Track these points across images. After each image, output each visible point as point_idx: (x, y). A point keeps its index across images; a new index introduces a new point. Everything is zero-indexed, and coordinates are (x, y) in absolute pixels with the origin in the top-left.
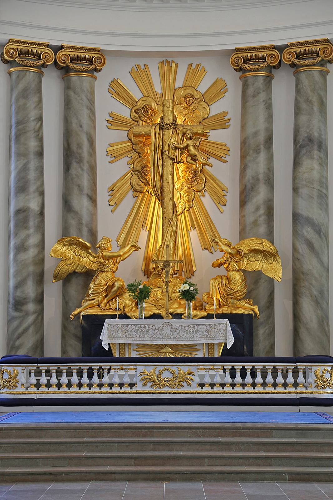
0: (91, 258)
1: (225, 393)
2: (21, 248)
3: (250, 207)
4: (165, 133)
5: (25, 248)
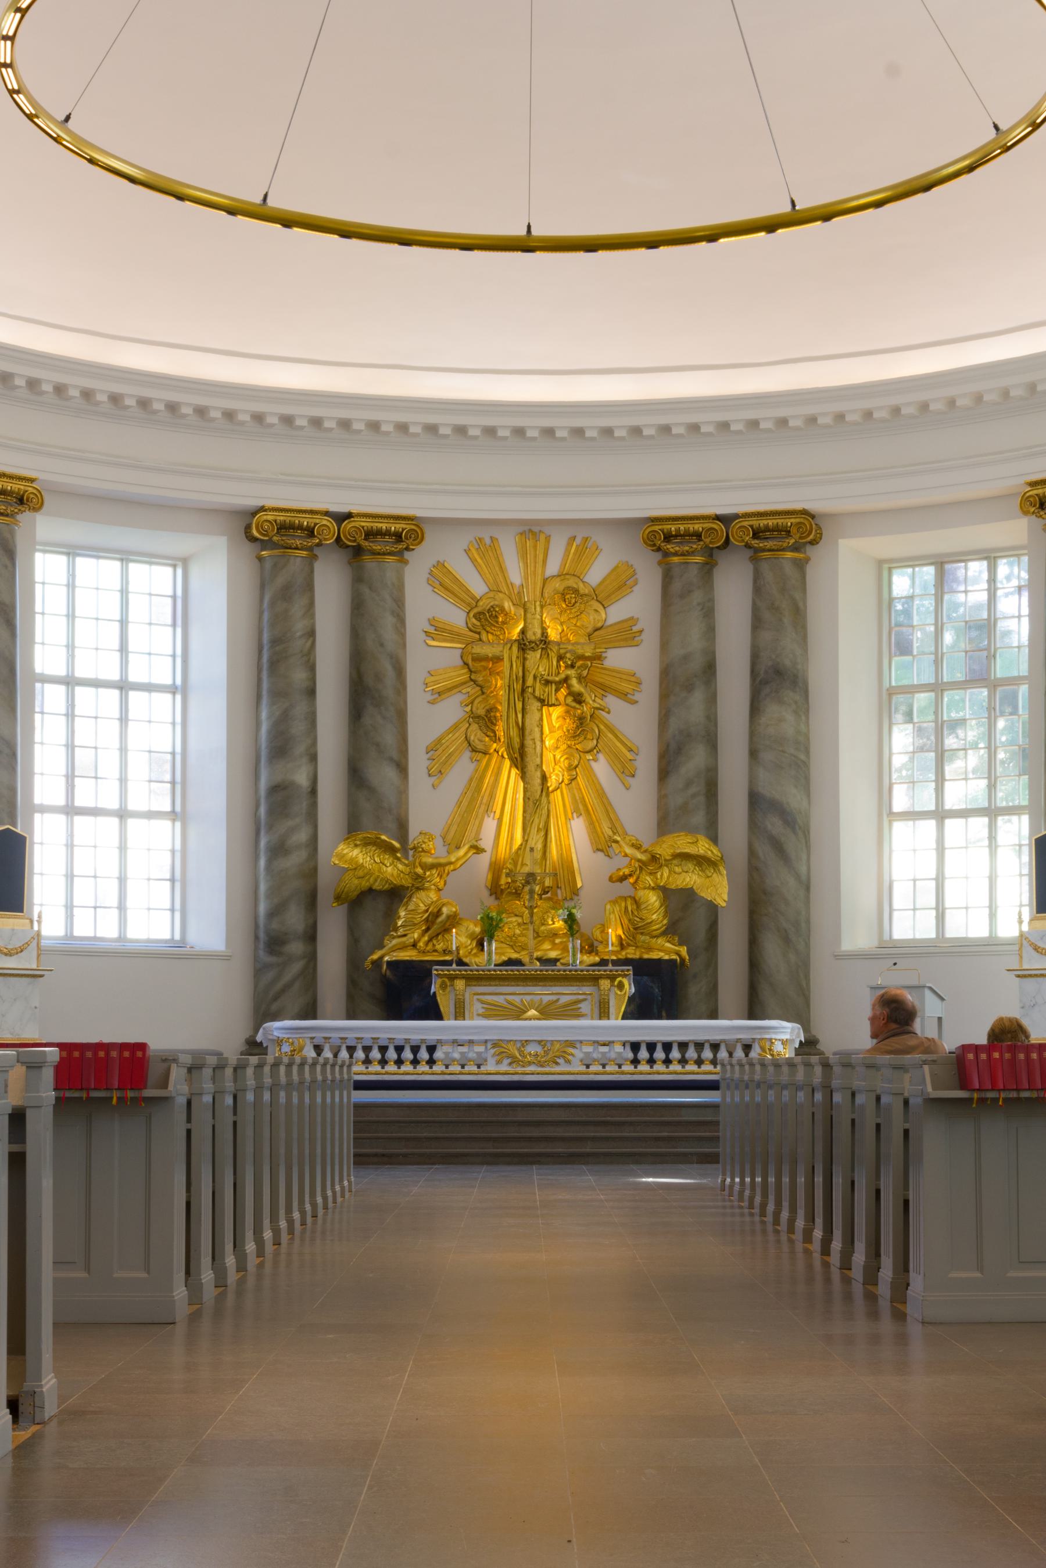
0: (400, 866)
1: (623, 1073)
2: (278, 850)
3: (675, 782)
4: (528, 656)
5: (286, 850)
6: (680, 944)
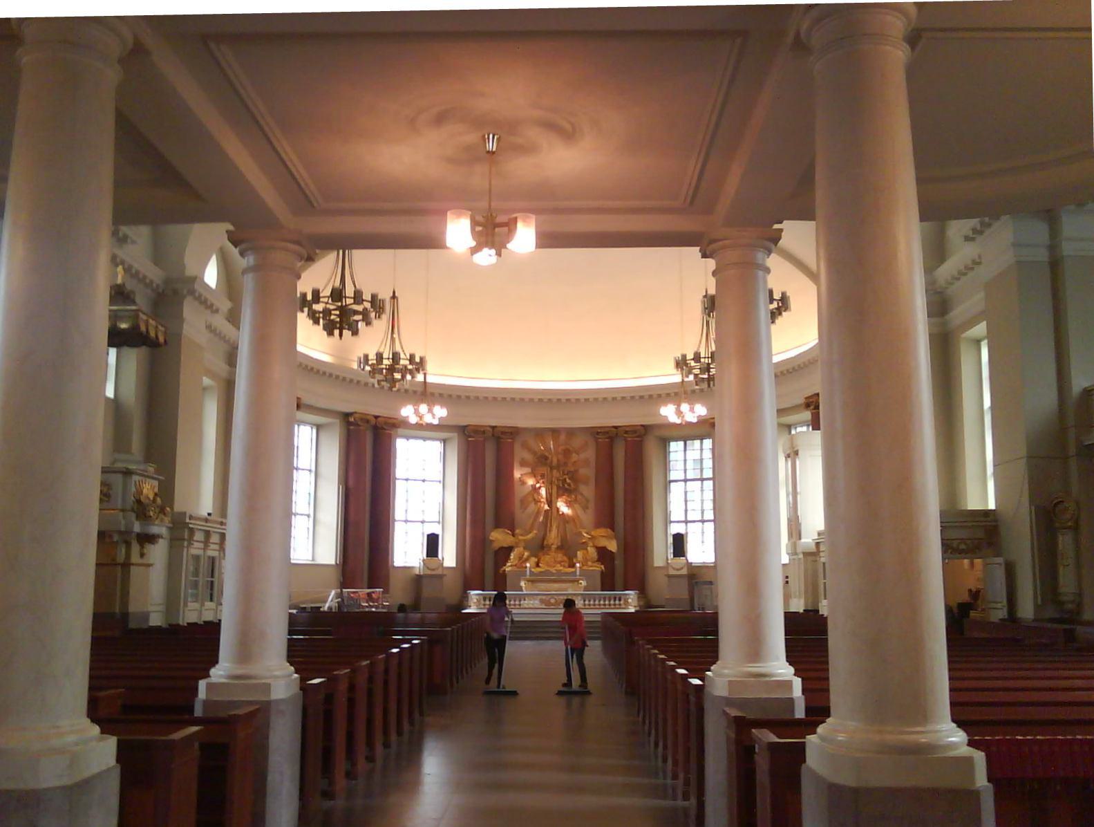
6: (602, 564)
